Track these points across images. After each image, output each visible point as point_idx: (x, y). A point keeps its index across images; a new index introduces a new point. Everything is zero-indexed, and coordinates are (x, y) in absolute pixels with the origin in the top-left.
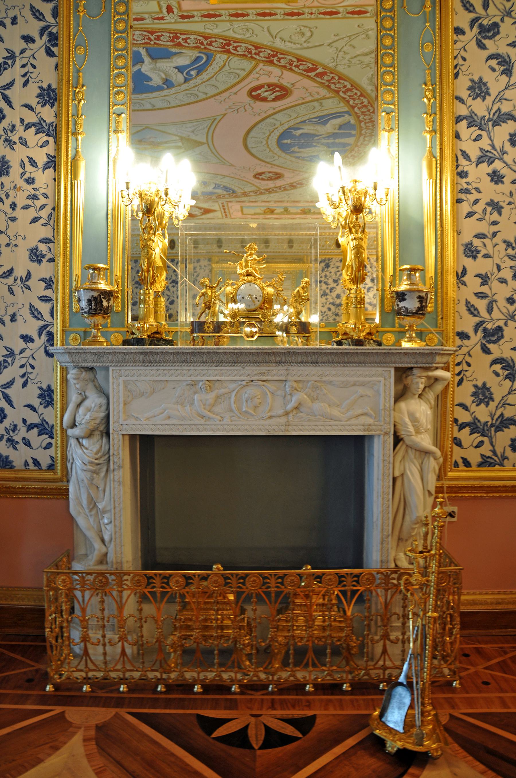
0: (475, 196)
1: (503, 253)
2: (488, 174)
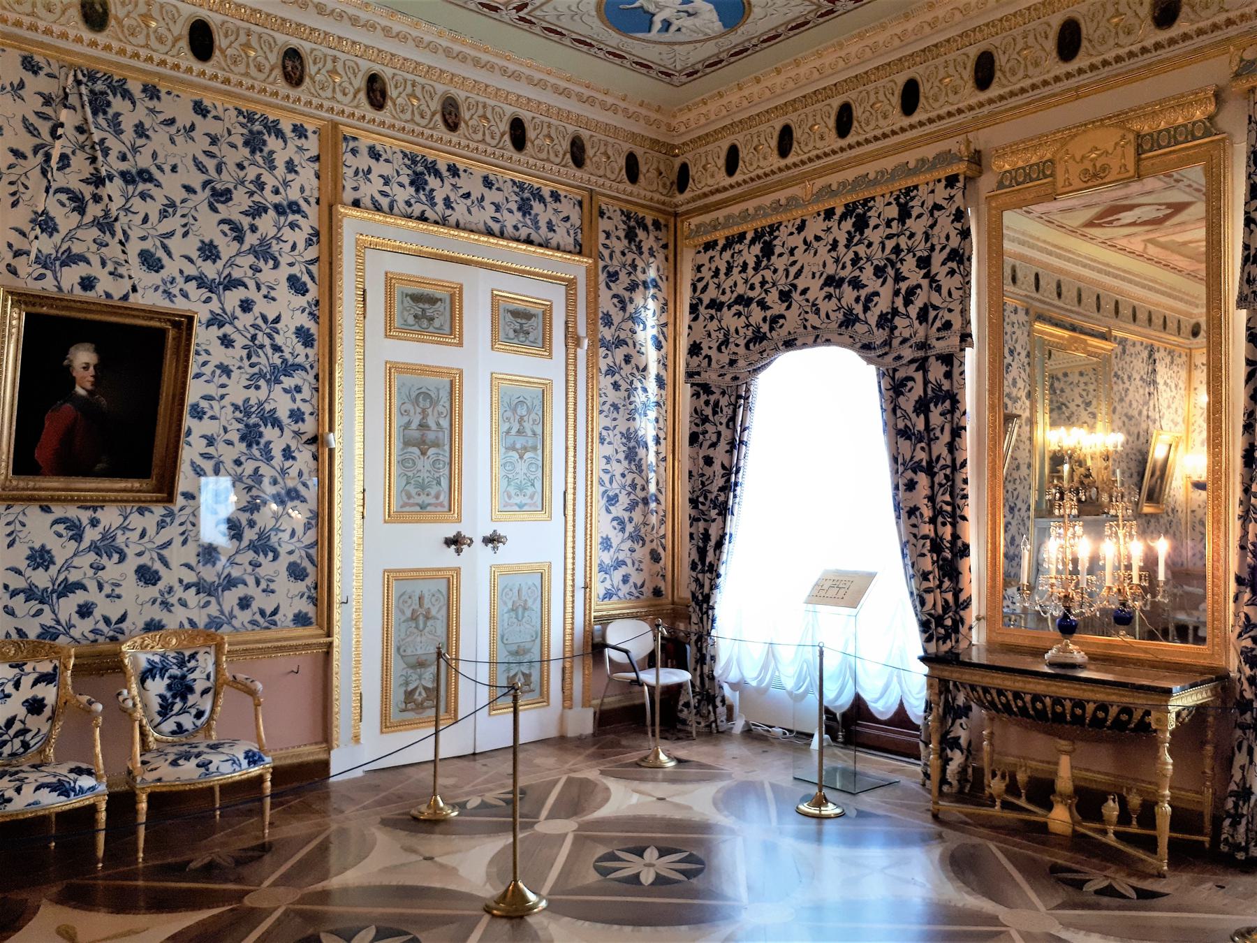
0: (204, 357)
1: (230, 416)
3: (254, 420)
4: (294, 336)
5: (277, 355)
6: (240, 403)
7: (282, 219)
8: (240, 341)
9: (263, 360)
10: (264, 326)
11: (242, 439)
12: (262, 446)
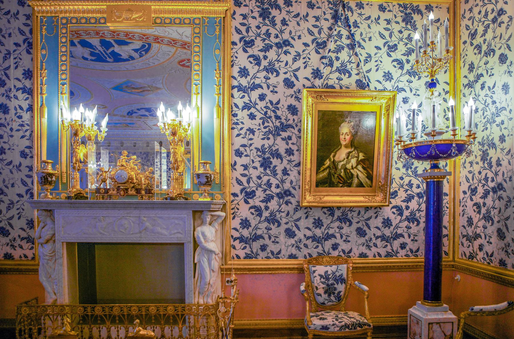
0: (241, 126)
1: (255, 154)
2: (248, 115)
3: (267, 155)
4: (286, 110)
5: (278, 121)
6: (260, 148)
7: (280, 50)
8: (259, 115)
9: (271, 124)
10: (271, 107)
11: (261, 166)
12: (271, 169)
